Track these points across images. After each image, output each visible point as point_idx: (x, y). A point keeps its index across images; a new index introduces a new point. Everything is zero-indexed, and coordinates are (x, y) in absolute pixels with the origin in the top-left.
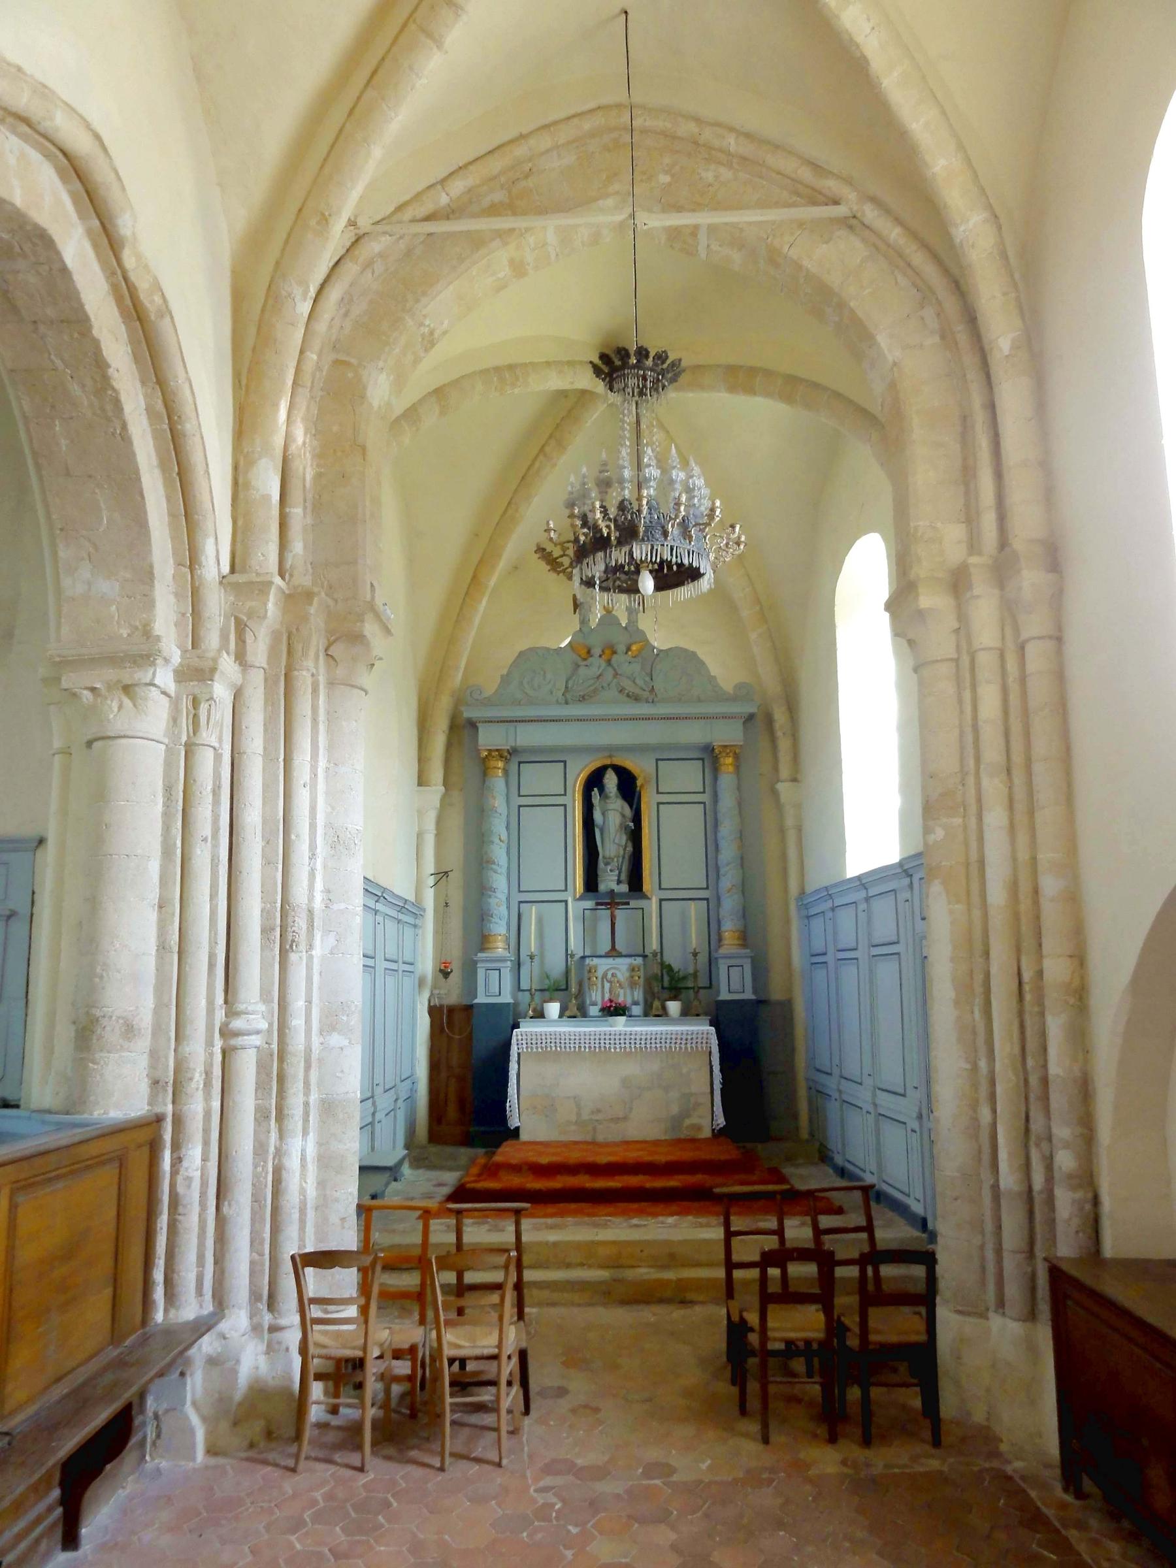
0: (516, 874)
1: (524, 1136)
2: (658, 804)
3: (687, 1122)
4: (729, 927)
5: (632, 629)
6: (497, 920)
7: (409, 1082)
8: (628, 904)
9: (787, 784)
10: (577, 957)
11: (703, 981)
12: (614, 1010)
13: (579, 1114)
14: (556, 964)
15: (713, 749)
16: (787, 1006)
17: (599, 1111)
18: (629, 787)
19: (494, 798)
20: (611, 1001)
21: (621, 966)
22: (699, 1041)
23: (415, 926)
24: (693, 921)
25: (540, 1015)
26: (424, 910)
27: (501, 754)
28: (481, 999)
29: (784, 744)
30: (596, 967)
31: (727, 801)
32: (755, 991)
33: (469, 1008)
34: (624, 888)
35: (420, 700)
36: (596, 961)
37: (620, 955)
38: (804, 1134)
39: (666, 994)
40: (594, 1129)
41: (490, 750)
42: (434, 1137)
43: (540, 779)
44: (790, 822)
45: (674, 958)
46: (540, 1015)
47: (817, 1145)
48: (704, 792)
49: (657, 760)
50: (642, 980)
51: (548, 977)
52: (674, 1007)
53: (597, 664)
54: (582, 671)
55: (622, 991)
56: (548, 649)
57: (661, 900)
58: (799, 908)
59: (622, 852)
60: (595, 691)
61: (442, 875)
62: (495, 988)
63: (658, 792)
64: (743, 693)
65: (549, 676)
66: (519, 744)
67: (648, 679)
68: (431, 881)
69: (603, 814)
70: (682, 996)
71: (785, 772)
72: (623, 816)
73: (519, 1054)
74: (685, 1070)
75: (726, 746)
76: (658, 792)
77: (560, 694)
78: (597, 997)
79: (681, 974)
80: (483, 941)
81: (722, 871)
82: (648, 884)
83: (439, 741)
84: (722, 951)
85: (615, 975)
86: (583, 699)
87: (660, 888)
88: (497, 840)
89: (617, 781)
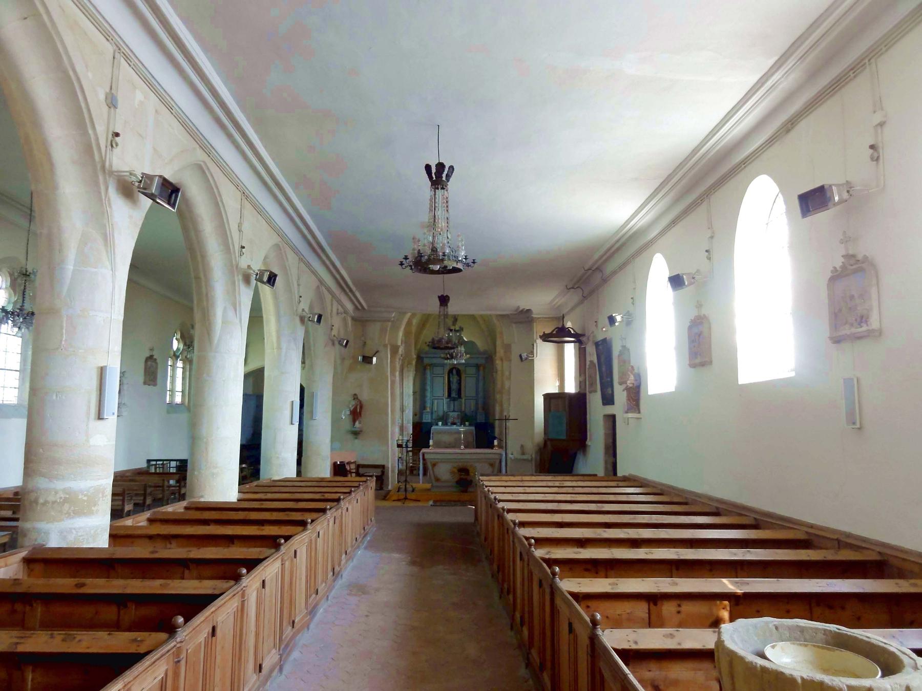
0: (432, 392)
12: (454, 424)
14: (441, 413)
18: (459, 373)
21: (455, 414)
25: (437, 425)
43: (438, 370)
45: (468, 411)
62: (427, 418)
64: (485, 352)
78: (450, 420)
80: (424, 408)
82: (463, 395)
85: (454, 415)
89: (455, 371)
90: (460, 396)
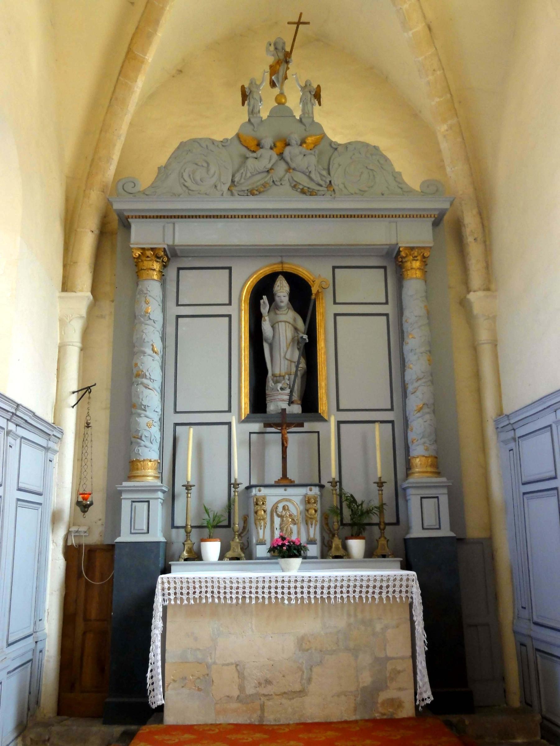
1: (170, 718)
2: (336, 315)
3: (383, 696)
4: (420, 452)
5: (306, 122)
6: (147, 443)
7: (30, 640)
8: (302, 425)
9: (481, 294)
10: (242, 487)
11: (389, 517)
12: (286, 550)
13: (242, 688)
14: (216, 495)
15: (399, 252)
16: (487, 547)
17: (268, 682)
18: (303, 297)
19: (147, 303)
20: (283, 538)
21: (296, 495)
22: (397, 589)
23: (47, 449)
24: (378, 448)
25: (196, 556)
26: (62, 433)
27: (156, 254)
28: (125, 537)
29: (475, 251)
30: (264, 498)
31: (415, 309)
32: (452, 530)
33: (112, 548)
34: (297, 409)
35: (67, 200)
36: (264, 491)
37: (292, 485)
38: (515, 701)
39: (347, 531)
40: (262, 708)
41: (143, 249)
42: (65, 707)
44: (484, 335)
45: (355, 487)
46: (196, 556)
47: (538, 718)
48: (387, 303)
49: (334, 268)
50: (318, 516)
51: (207, 511)
52: (356, 546)
53: (267, 158)
54: (251, 163)
55: (294, 528)
56: (213, 142)
57: (339, 423)
58: (499, 429)
59: (294, 369)
60: (264, 185)
61: (85, 391)
62: (144, 523)
63: (335, 303)
64: (433, 188)
65: (213, 169)
66: (177, 242)
67: (324, 173)
68: (73, 399)
69: (273, 327)
70: (365, 534)
71: (476, 279)
72: (296, 329)
73: (165, 608)
74: (378, 627)
75: (412, 248)
76: (335, 303)
77: (225, 188)
78: (265, 535)
79: (365, 506)
81: (410, 388)
83: (87, 243)
84: (414, 479)
85: (287, 507)
86: (252, 193)
87: (338, 409)
88: (149, 351)
90: (309, 402)
